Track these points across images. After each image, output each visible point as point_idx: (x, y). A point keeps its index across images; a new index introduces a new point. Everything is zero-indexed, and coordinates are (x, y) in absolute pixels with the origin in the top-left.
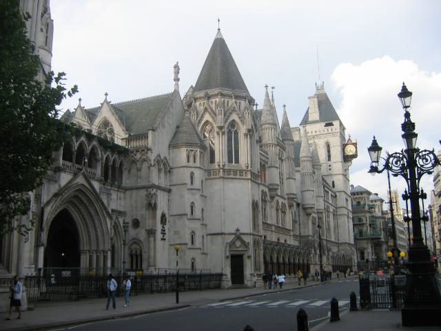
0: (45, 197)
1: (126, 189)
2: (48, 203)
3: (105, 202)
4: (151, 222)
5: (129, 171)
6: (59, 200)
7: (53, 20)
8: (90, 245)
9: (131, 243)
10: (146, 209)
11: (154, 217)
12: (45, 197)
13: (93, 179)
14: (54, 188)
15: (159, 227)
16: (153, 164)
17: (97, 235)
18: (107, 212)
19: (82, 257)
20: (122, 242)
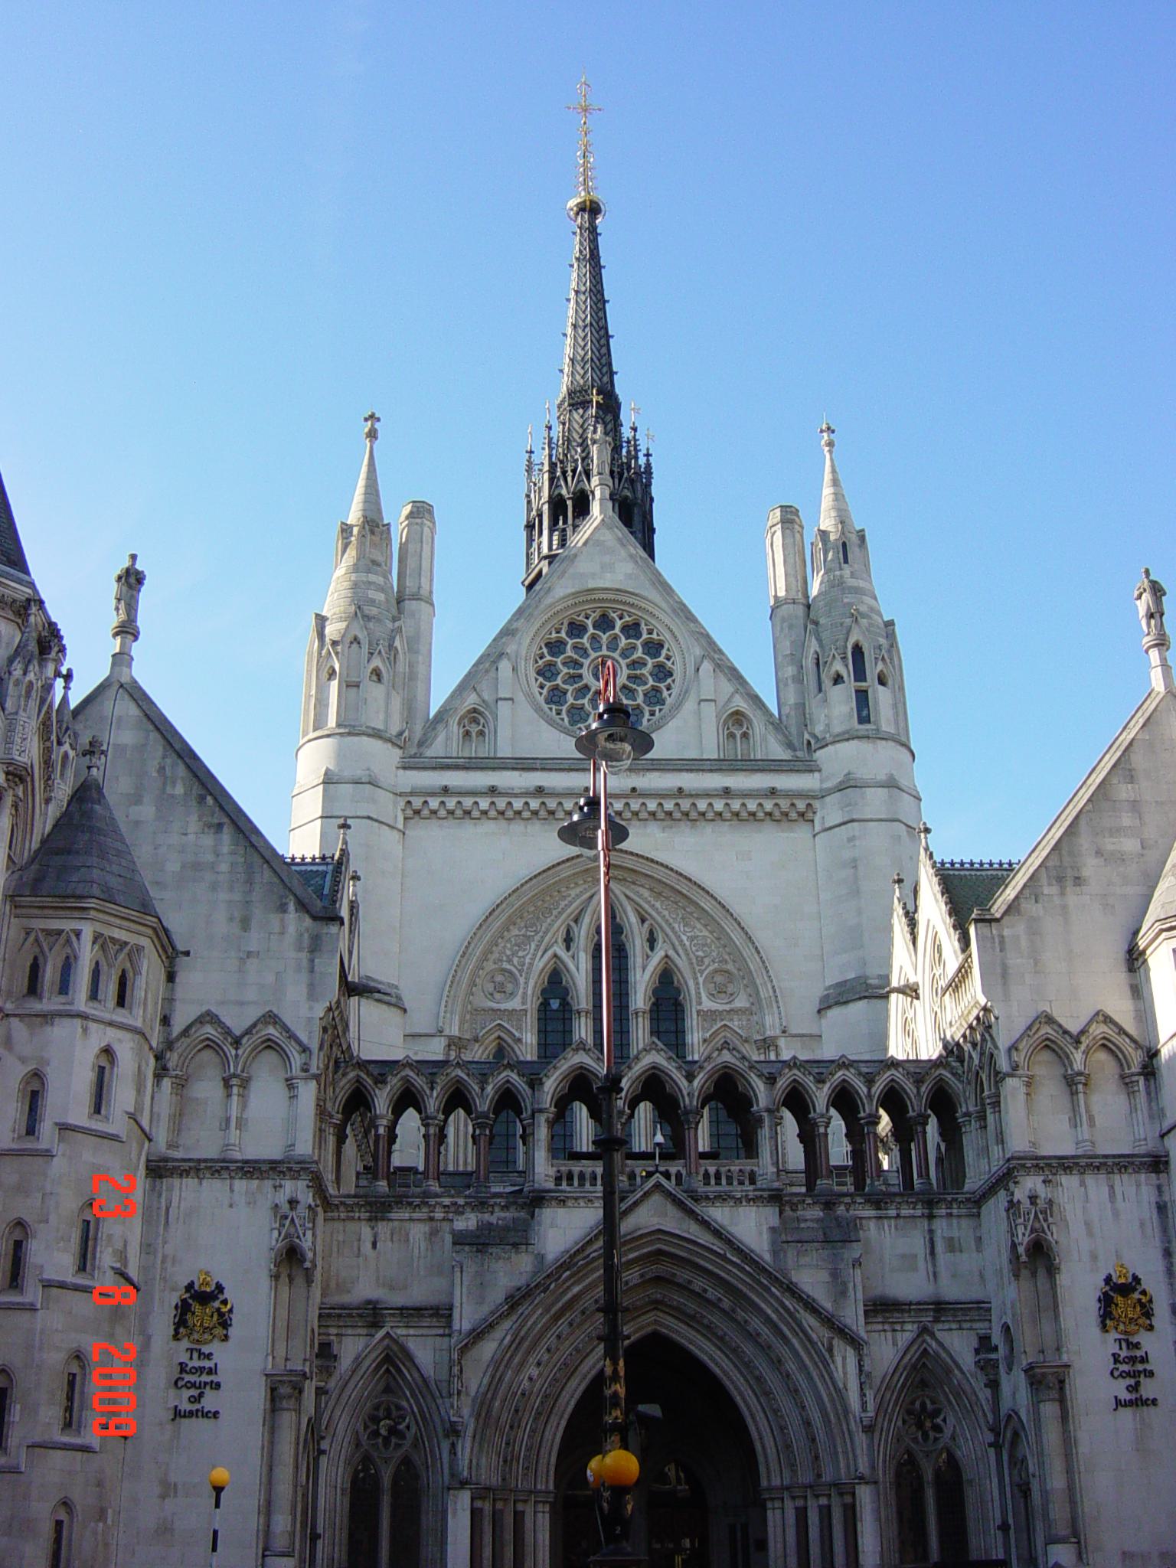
0: (468, 1309)
1: (978, 1201)
2: (478, 1335)
3: (811, 1279)
4: (1047, 1327)
5: (982, 1117)
6: (535, 1315)
7: (890, 624)
8: (792, 1466)
9: (1009, 1435)
10: (1017, 1276)
11: (1050, 1305)
12: (468, 1309)
13: (722, 1198)
14: (510, 1271)
15: (1089, 1350)
16: (1003, 1065)
17: (808, 1424)
18: (829, 1321)
19: (769, 1513)
20: (990, 1437)
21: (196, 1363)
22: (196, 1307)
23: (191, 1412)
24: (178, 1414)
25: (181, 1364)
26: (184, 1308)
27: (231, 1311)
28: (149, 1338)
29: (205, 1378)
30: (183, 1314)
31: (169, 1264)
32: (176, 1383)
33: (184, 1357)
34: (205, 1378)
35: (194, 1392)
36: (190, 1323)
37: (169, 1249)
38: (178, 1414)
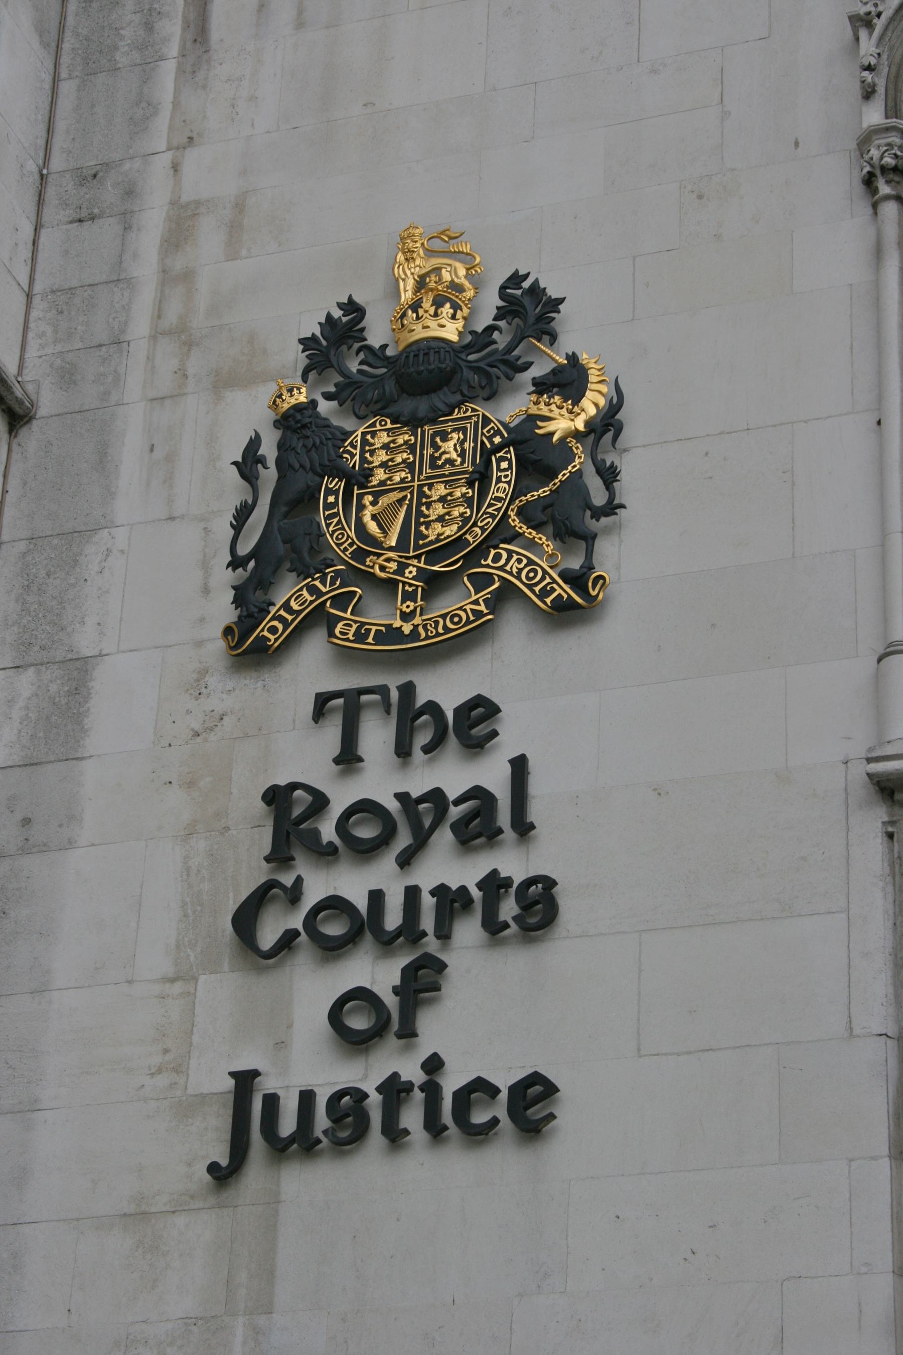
21: (381, 780)
22: (379, 444)
23: (349, 1121)
24: (260, 1132)
25: (277, 797)
26: (300, 467)
27: (607, 425)
28: (79, 672)
29: (446, 866)
30: (296, 502)
31: (209, 240)
32: (245, 920)
33: (305, 757)
34: (446, 866)
35: (379, 973)
36: (339, 538)
37: (207, 175)
38: (260, 1132)
